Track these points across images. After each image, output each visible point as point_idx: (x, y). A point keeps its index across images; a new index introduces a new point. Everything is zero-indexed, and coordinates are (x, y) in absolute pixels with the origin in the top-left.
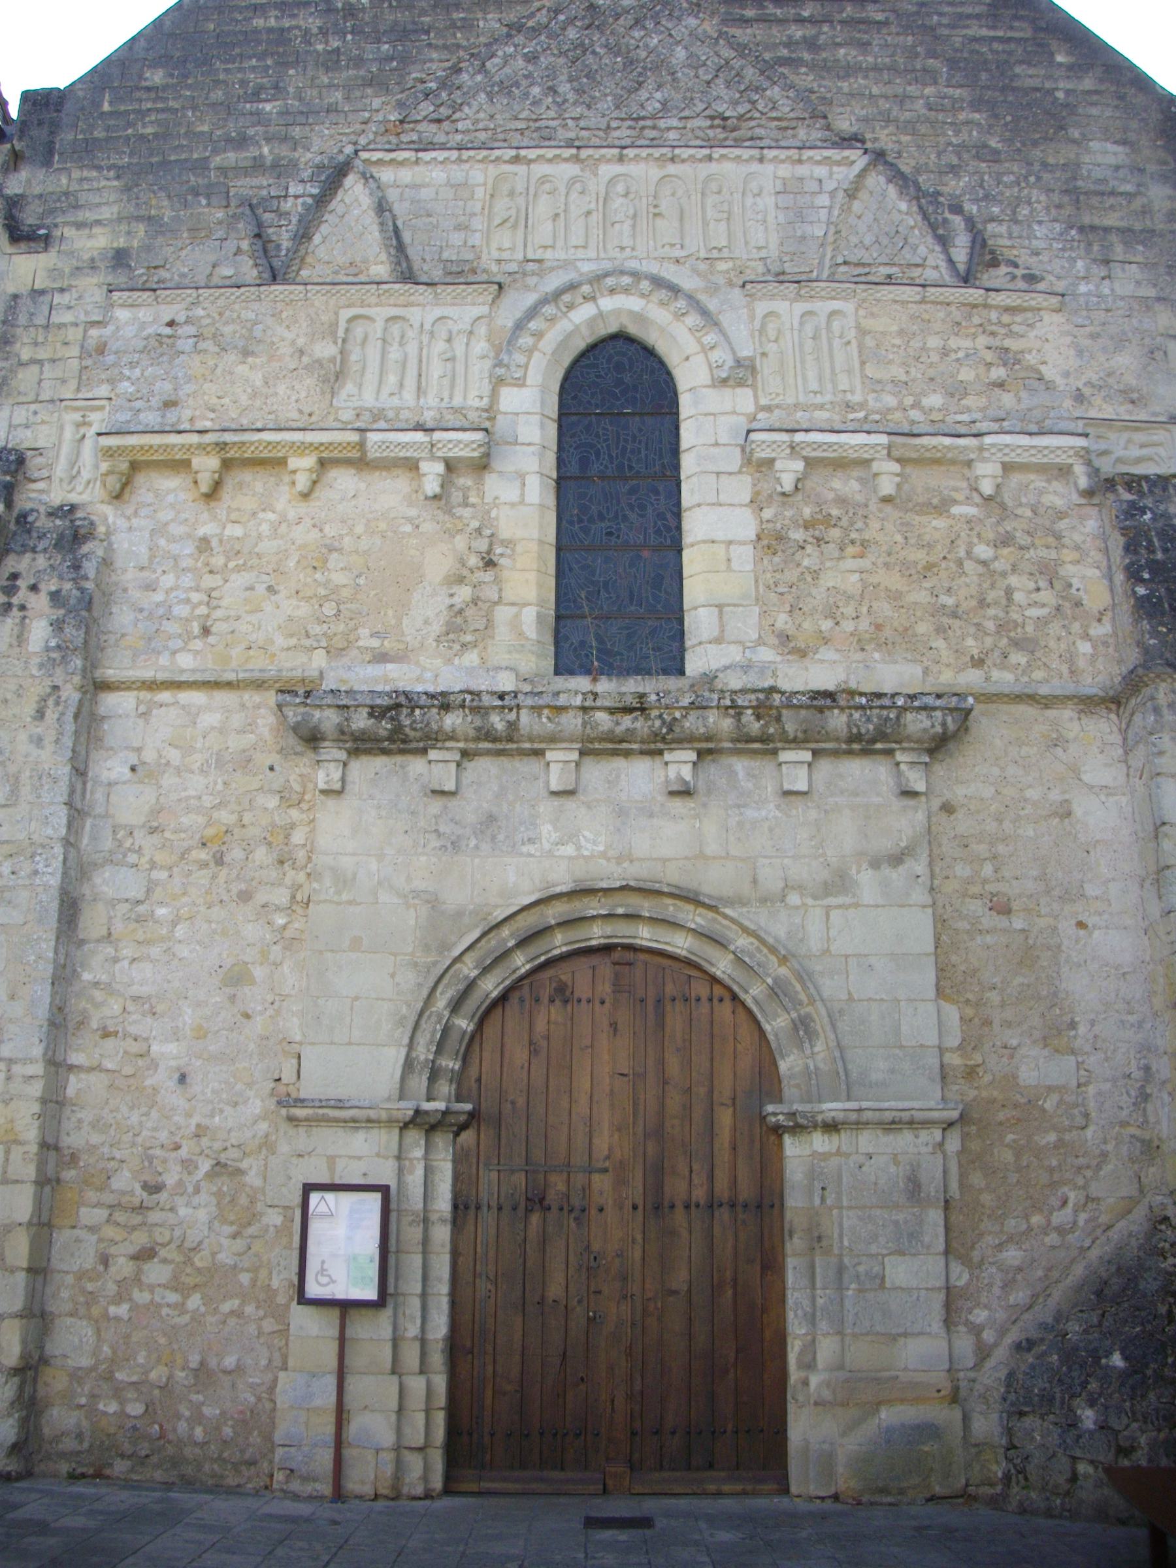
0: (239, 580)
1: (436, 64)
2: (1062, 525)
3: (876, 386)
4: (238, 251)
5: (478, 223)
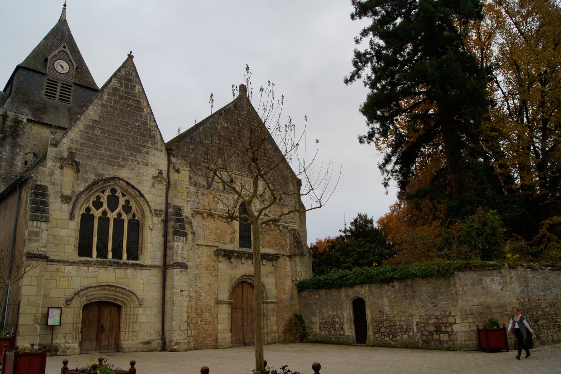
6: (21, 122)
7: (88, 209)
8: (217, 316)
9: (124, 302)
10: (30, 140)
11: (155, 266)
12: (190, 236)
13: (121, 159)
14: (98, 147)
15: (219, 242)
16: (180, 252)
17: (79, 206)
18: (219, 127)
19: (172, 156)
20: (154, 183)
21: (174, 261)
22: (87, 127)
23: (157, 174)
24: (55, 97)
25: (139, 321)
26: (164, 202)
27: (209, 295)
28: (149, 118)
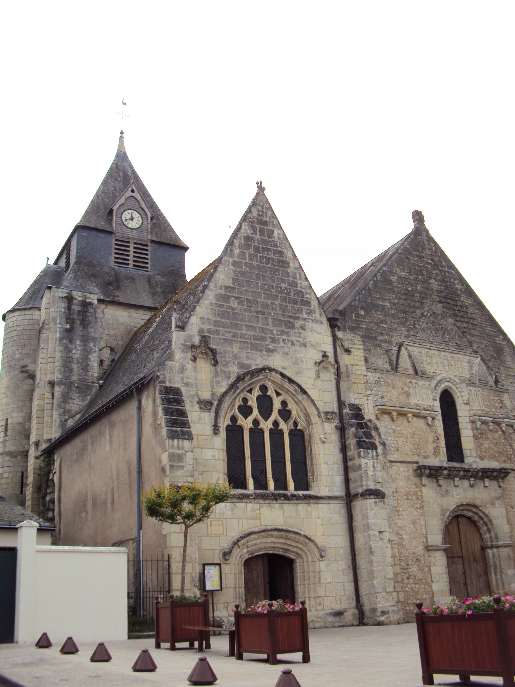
0: (402, 439)
1: (410, 322)
2: (512, 436)
3: (486, 406)
4: (387, 362)
5: (425, 362)
6: (91, 304)
7: (234, 419)
8: (430, 570)
9: (298, 554)
10: (104, 329)
11: (336, 498)
12: (380, 448)
13: (269, 340)
14: (236, 325)
15: (418, 456)
16: (370, 473)
17: (222, 413)
18: (394, 278)
19: (336, 329)
20: (318, 372)
21: (365, 488)
22: (219, 297)
23: (321, 358)
24: (128, 264)
25: (322, 581)
26: (335, 399)
27: (415, 538)
28: (298, 275)
